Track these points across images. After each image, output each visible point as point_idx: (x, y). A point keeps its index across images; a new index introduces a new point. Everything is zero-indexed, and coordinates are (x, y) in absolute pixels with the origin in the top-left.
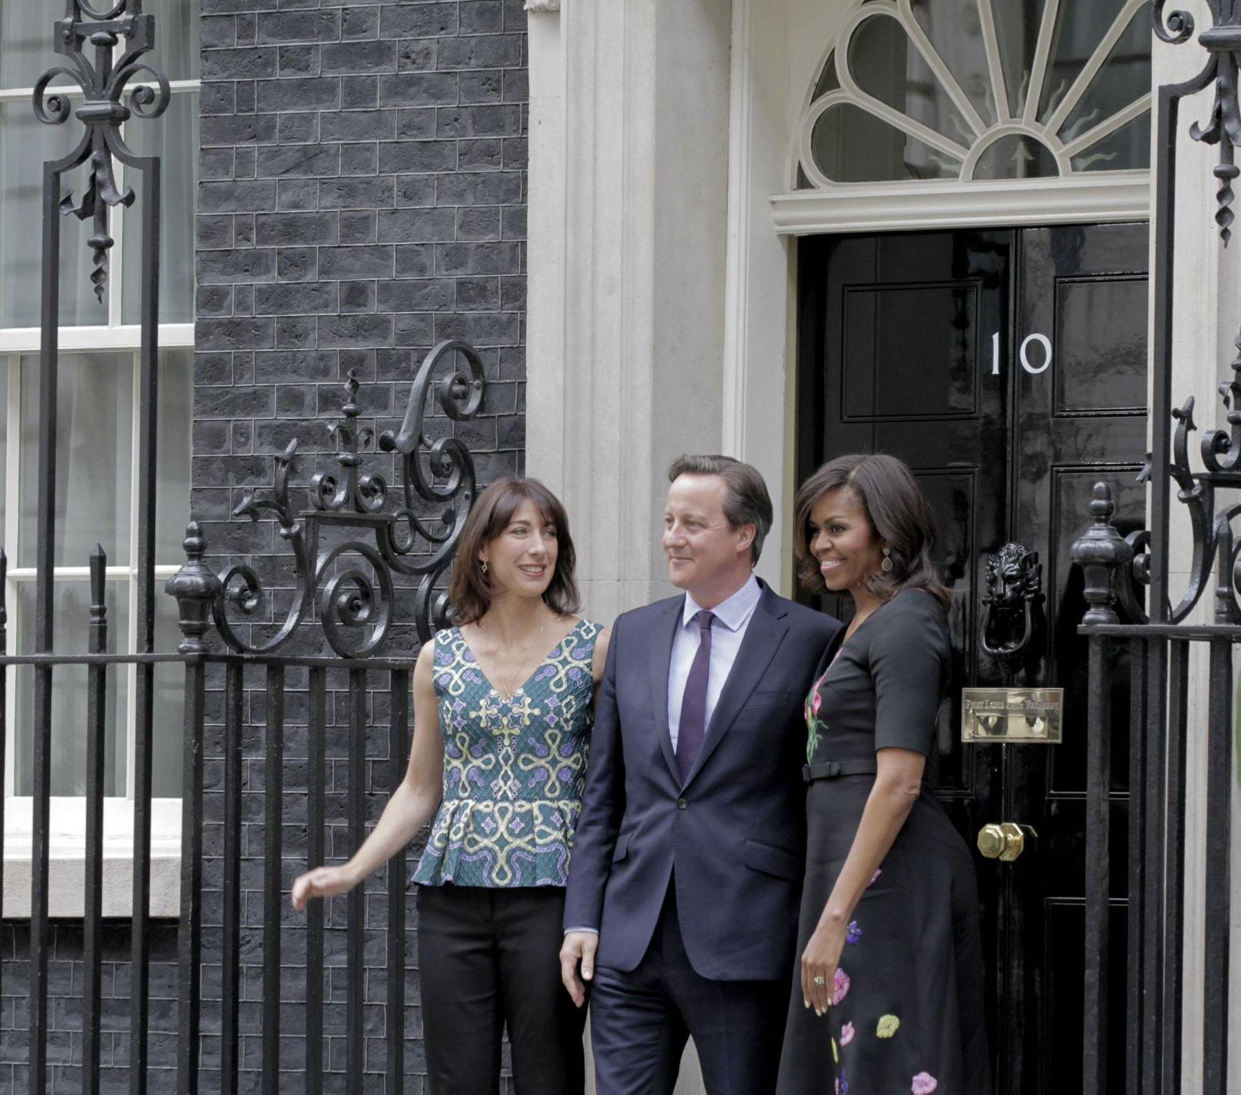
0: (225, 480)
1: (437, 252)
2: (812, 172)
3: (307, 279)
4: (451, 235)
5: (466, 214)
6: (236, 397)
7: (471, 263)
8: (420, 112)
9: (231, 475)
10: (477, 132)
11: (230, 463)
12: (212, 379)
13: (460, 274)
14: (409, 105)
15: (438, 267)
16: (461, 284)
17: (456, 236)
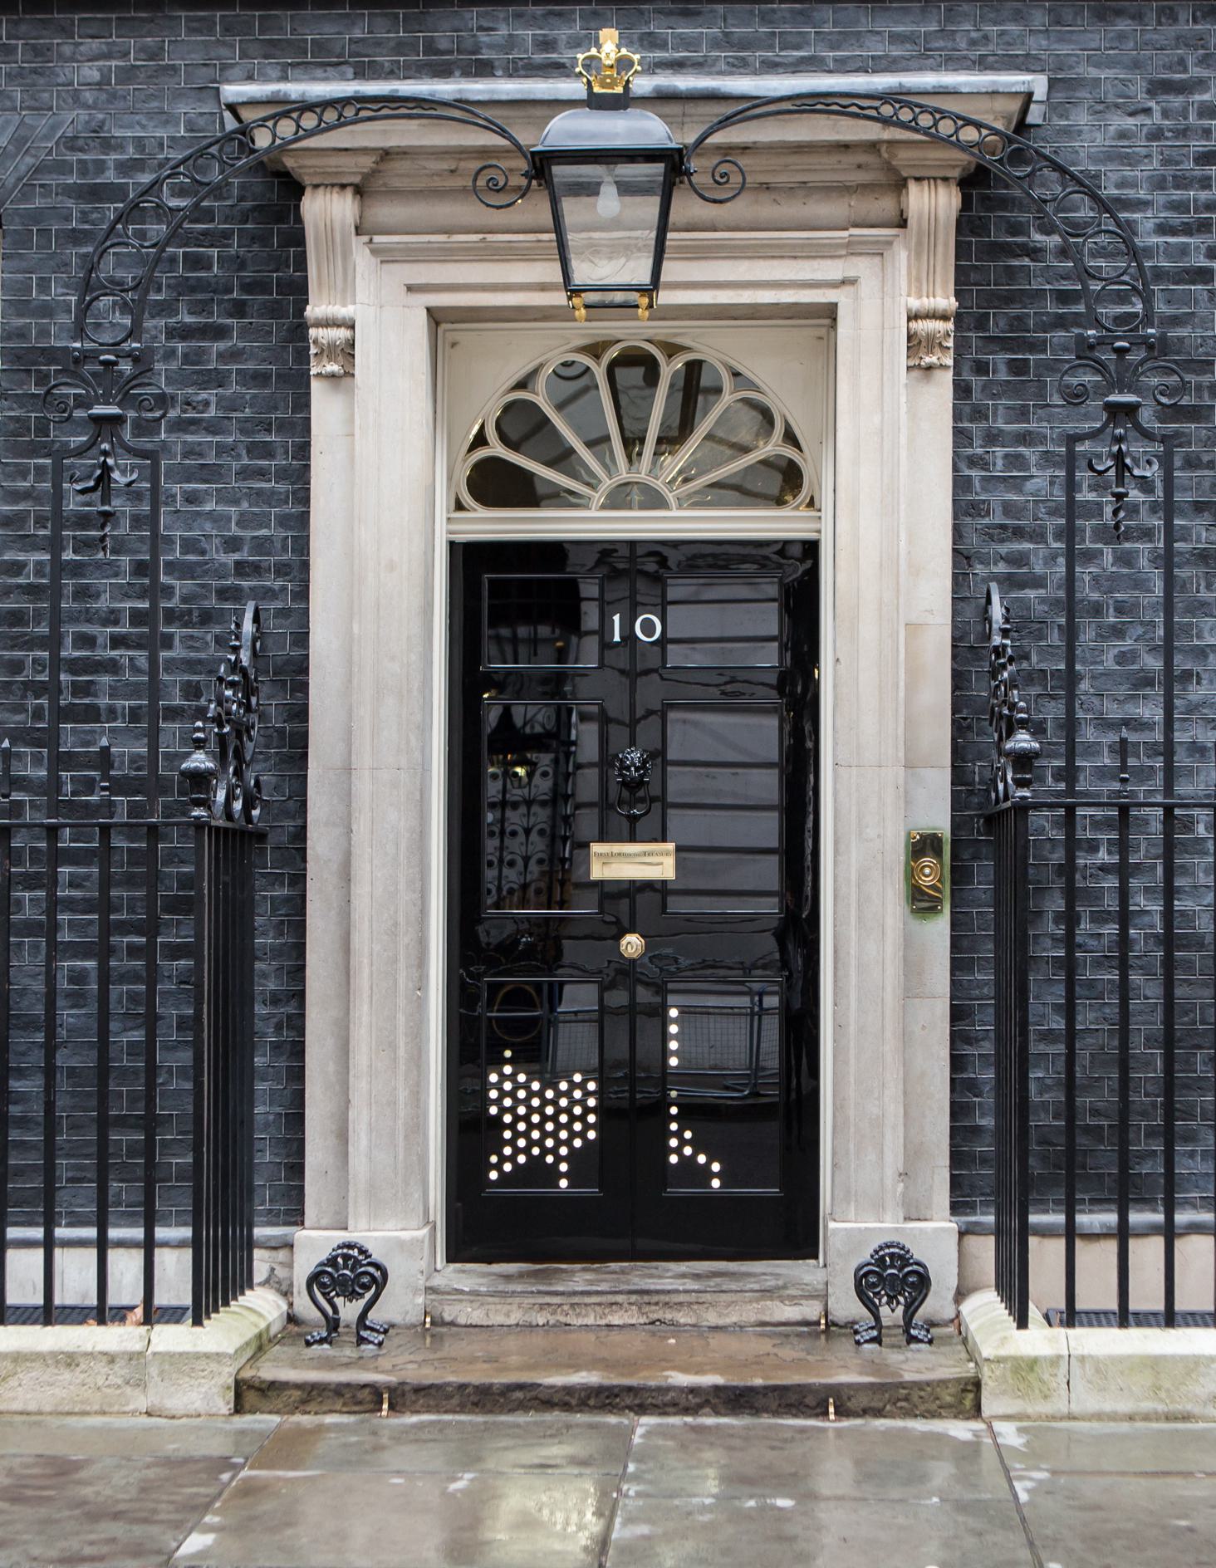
0: (24, 697)
1: (216, 541)
2: (467, 499)
3: (101, 555)
4: (230, 530)
5: (242, 514)
6: (32, 639)
7: (246, 549)
8: (200, 444)
9: (29, 693)
10: (251, 459)
11: (27, 685)
12: (11, 625)
13: (237, 556)
14: (189, 438)
15: (217, 551)
16: (238, 563)
17: (234, 530)
